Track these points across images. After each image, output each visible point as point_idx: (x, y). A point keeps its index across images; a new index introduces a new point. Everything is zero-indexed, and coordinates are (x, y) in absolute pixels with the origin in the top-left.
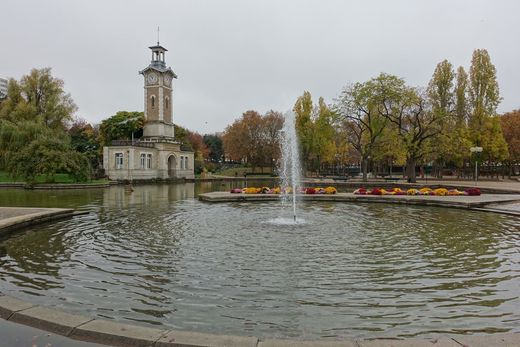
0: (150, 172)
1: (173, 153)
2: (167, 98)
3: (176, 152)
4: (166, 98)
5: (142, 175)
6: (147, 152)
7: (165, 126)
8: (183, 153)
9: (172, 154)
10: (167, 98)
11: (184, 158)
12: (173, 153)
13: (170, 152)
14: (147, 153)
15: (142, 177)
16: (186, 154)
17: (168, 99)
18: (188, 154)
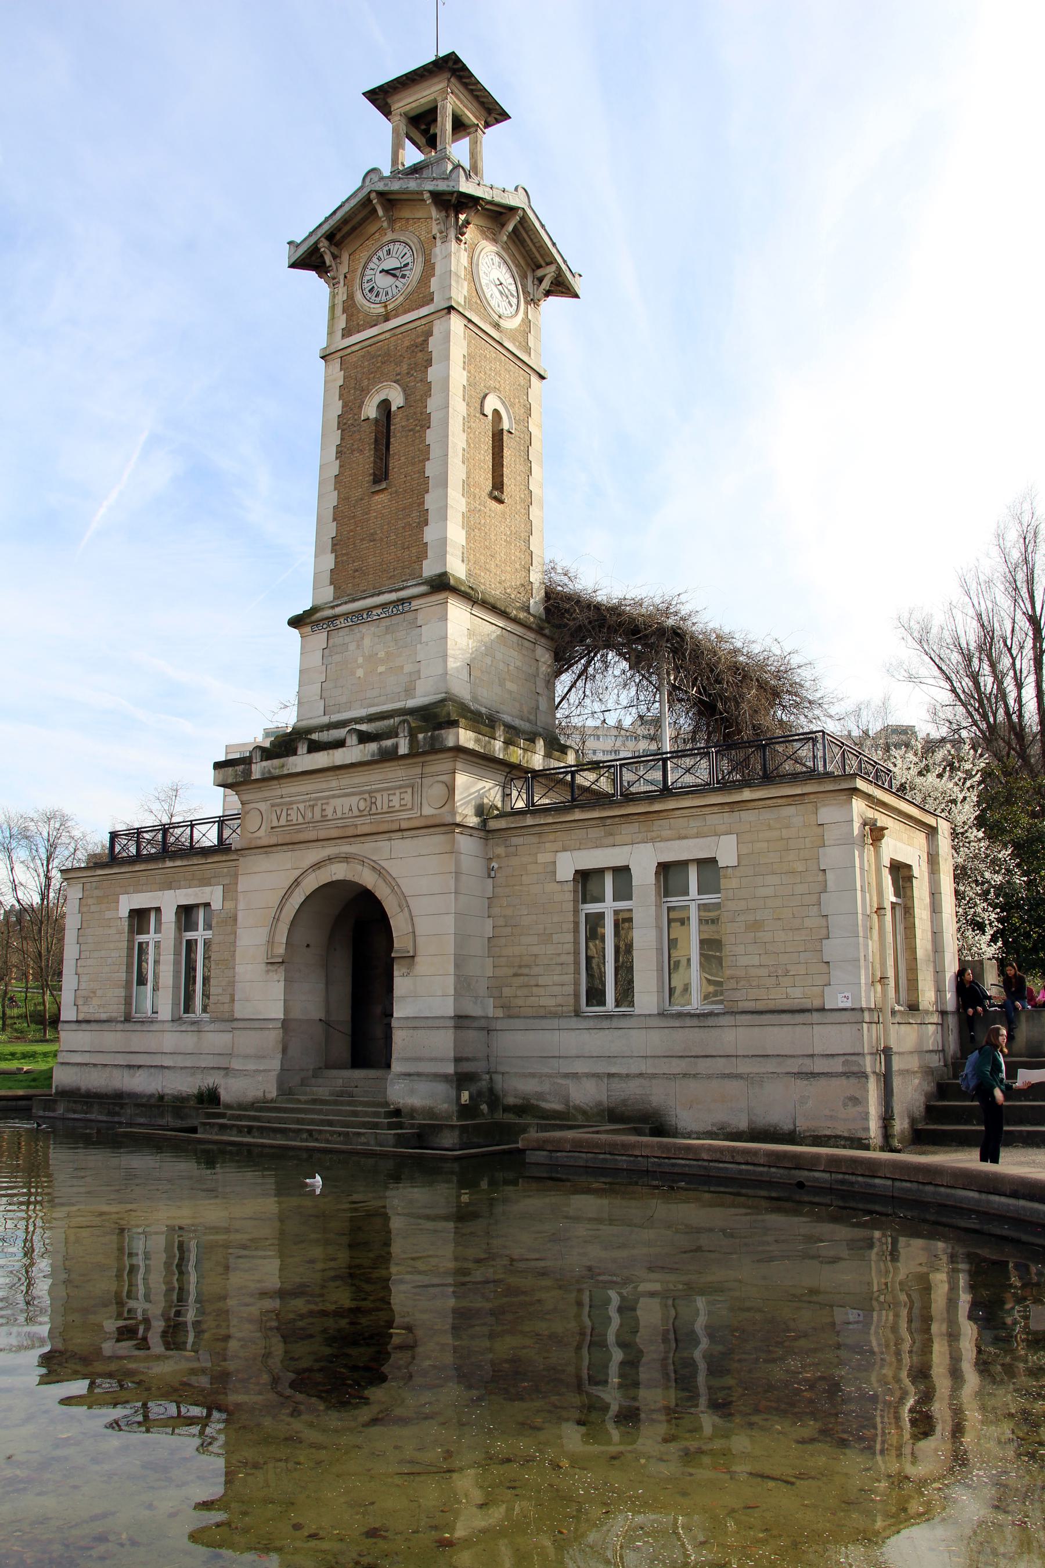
0: (188, 1041)
1: (346, 859)
2: (385, 405)
3: (401, 846)
4: (370, 410)
5: (121, 1060)
6: (169, 894)
7: (338, 638)
8: (629, 830)
9: (338, 872)
10: (385, 405)
11: (644, 876)
12: (346, 859)
13: (314, 855)
14: (169, 901)
15: (117, 1073)
16: (661, 826)
17: (397, 399)
18: (716, 820)
